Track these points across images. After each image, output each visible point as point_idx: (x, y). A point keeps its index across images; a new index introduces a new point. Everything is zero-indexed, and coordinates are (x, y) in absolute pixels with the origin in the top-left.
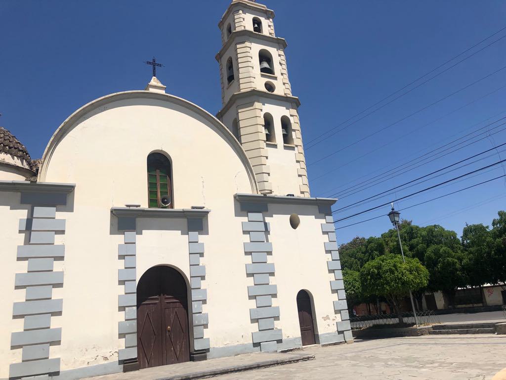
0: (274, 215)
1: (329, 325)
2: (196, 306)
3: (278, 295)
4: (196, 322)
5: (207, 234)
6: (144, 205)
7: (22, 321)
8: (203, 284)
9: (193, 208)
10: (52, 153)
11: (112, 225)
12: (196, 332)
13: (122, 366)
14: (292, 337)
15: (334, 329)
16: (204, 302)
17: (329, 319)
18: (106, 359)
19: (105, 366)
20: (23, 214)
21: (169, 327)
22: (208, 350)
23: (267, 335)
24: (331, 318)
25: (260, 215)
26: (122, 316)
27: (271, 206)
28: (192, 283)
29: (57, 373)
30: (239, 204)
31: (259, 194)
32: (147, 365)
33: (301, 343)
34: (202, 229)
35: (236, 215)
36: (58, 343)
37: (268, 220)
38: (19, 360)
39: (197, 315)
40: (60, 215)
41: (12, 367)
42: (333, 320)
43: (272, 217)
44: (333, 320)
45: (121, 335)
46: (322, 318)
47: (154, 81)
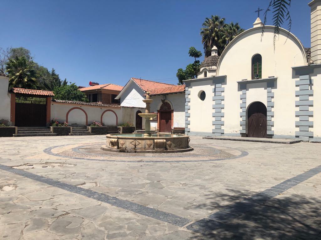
0: (317, 75)
2: (268, 118)
3: (314, 116)
4: (268, 124)
5: (276, 88)
6: (249, 79)
7: (214, 118)
9: (269, 77)
10: (220, 65)
11: (238, 87)
12: (268, 128)
13: (241, 135)
16: (273, 116)
18: (236, 132)
19: (236, 134)
20: (213, 87)
22: (273, 135)
23: (304, 133)
25: (308, 76)
26: (241, 119)
27: (315, 70)
28: (268, 109)
29: (223, 133)
30: (295, 71)
31: (307, 64)
34: (274, 86)
35: (293, 77)
36: (223, 125)
37: (312, 77)
38: (214, 129)
40: (223, 86)
41: (213, 130)
43: (317, 76)
45: (241, 125)
47: (258, 21)
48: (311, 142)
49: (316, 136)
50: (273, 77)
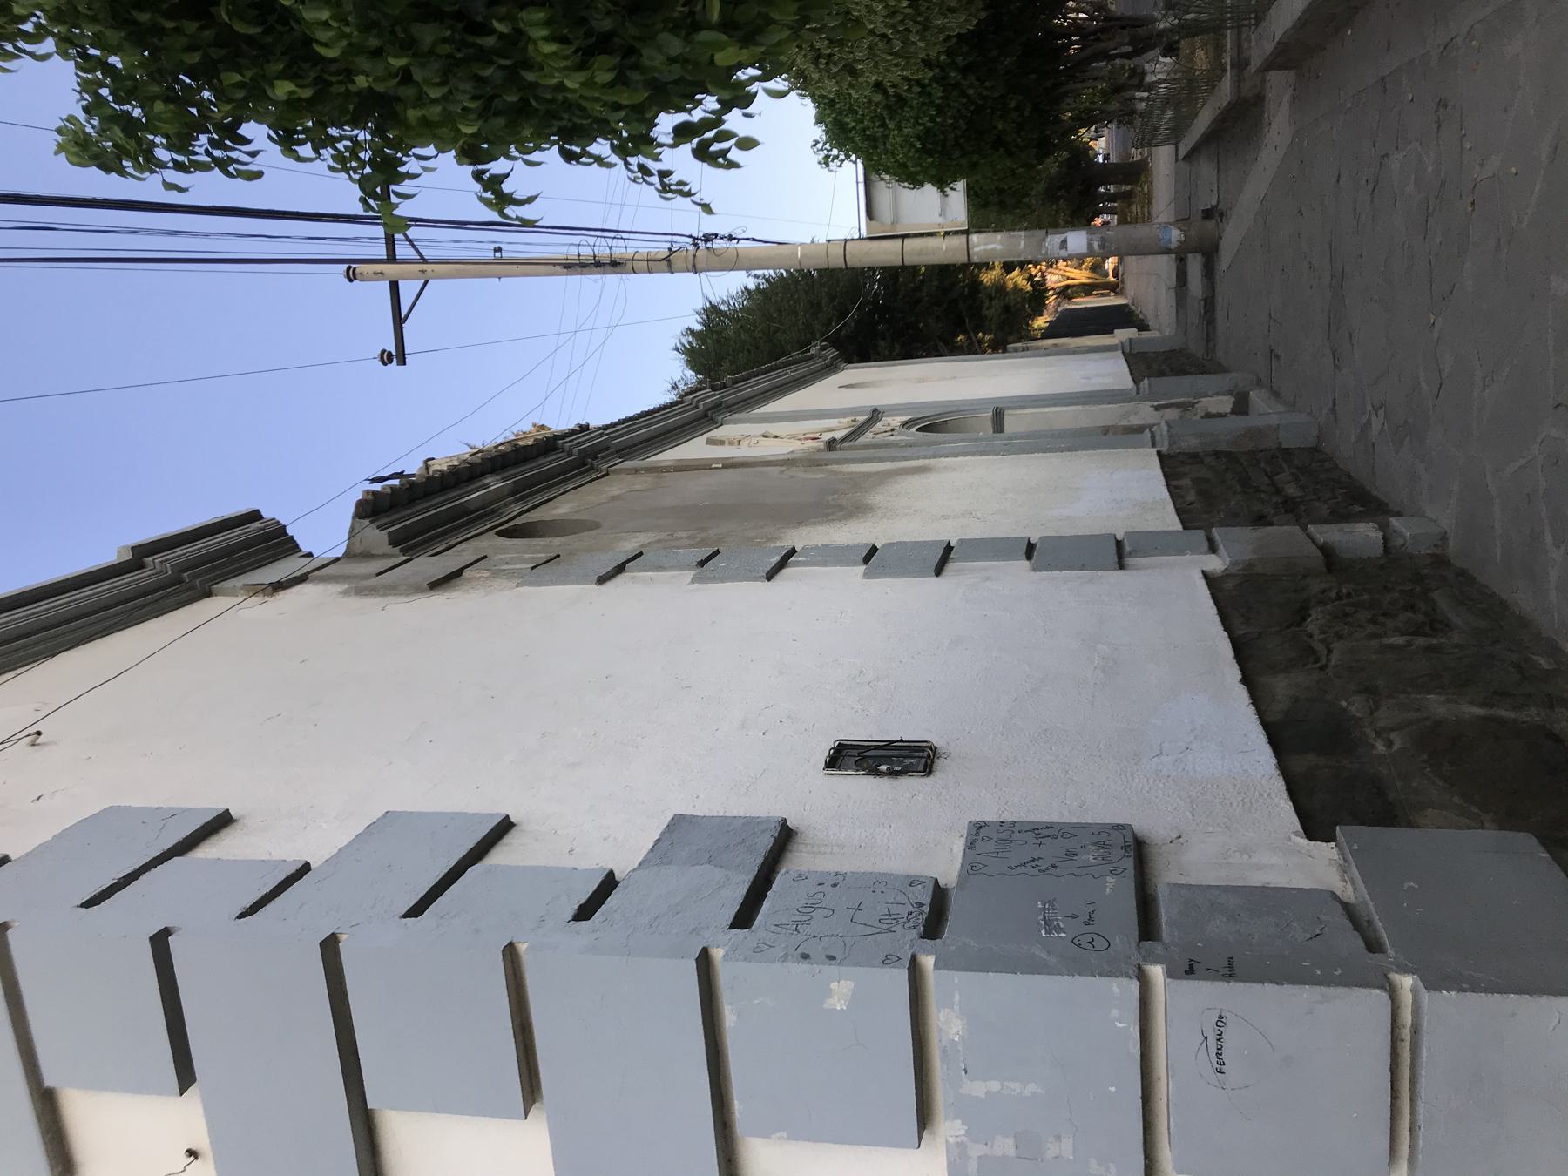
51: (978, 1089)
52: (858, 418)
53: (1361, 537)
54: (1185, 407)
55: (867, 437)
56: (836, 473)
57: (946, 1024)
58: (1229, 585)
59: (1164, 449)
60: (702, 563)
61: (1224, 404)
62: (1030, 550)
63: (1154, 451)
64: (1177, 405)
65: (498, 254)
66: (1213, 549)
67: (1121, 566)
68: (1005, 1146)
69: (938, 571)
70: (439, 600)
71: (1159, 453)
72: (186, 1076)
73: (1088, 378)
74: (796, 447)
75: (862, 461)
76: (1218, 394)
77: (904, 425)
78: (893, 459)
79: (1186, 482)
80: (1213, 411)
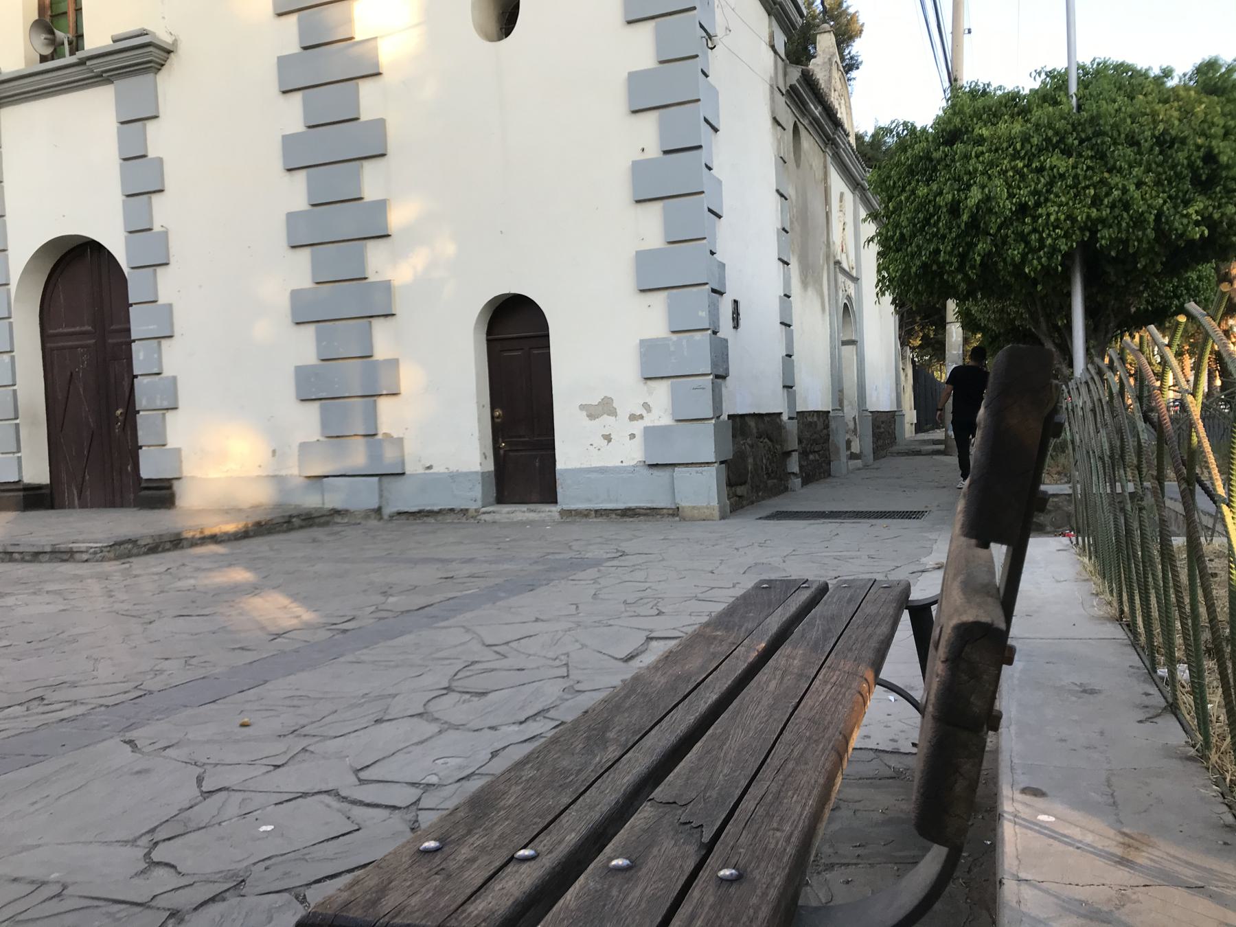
1: (608, 438)
2: (141, 357)
4: (141, 401)
8: (168, 286)
14: (442, 470)
15: (629, 453)
17: (613, 413)
21: (119, 412)
24: (623, 414)
32: (76, 502)
33: (478, 492)
39: (146, 380)
42: (633, 417)
44: (633, 417)
46: (582, 407)
48: (391, 517)
49: (423, 471)
50: (144, 33)
51: (684, 342)
52: (854, 270)
53: (794, 465)
54: (855, 431)
55: (841, 278)
56: (823, 269)
57: (698, 336)
58: (778, 420)
59: (831, 414)
60: (784, 229)
61: (855, 448)
62: (790, 356)
63: (830, 410)
64: (855, 428)
65: (967, 31)
66: (790, 418)
67: (784, 387)
68: (672, 349)
69: (782, 323)
70: (768, 122)
71: (829, 412)
72: (666, 152)
73: (876, 389)
74: (836, 236)
75: (829, 280)
76: (861, 446)
77: (849, 298)
78: (829, 295)
79: (815, 419)
80: (853, 444)
